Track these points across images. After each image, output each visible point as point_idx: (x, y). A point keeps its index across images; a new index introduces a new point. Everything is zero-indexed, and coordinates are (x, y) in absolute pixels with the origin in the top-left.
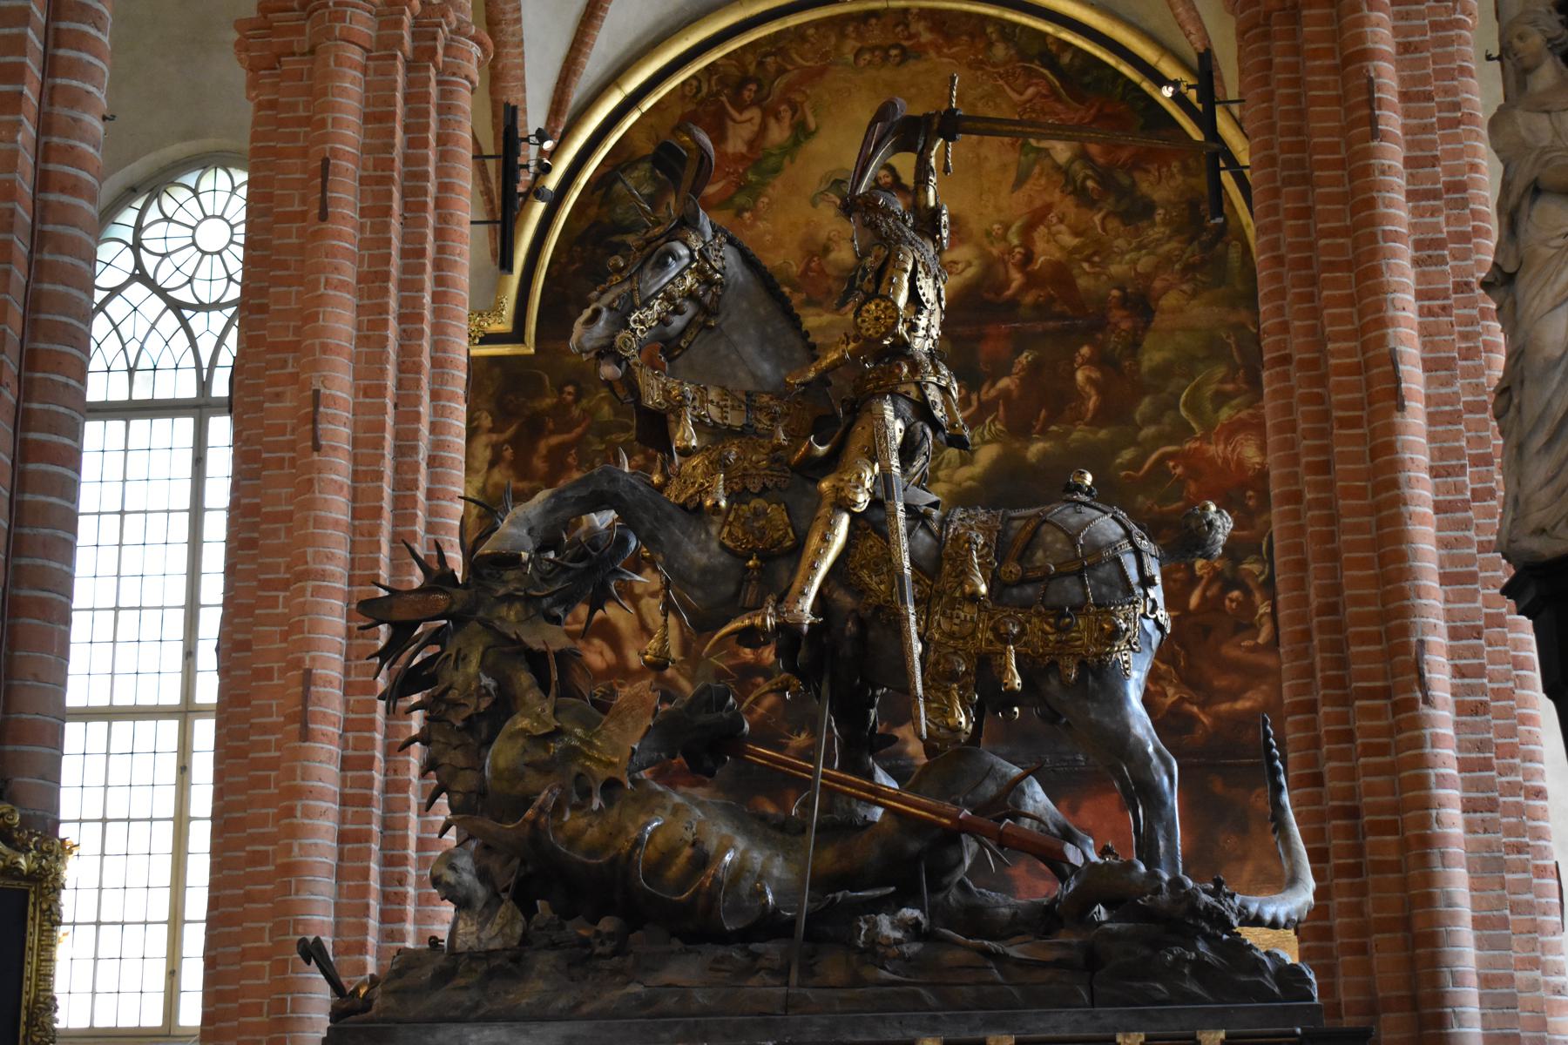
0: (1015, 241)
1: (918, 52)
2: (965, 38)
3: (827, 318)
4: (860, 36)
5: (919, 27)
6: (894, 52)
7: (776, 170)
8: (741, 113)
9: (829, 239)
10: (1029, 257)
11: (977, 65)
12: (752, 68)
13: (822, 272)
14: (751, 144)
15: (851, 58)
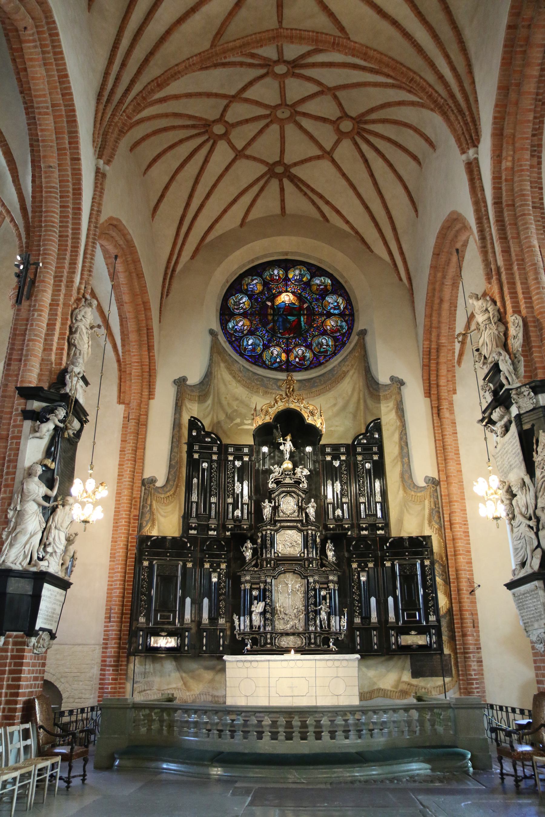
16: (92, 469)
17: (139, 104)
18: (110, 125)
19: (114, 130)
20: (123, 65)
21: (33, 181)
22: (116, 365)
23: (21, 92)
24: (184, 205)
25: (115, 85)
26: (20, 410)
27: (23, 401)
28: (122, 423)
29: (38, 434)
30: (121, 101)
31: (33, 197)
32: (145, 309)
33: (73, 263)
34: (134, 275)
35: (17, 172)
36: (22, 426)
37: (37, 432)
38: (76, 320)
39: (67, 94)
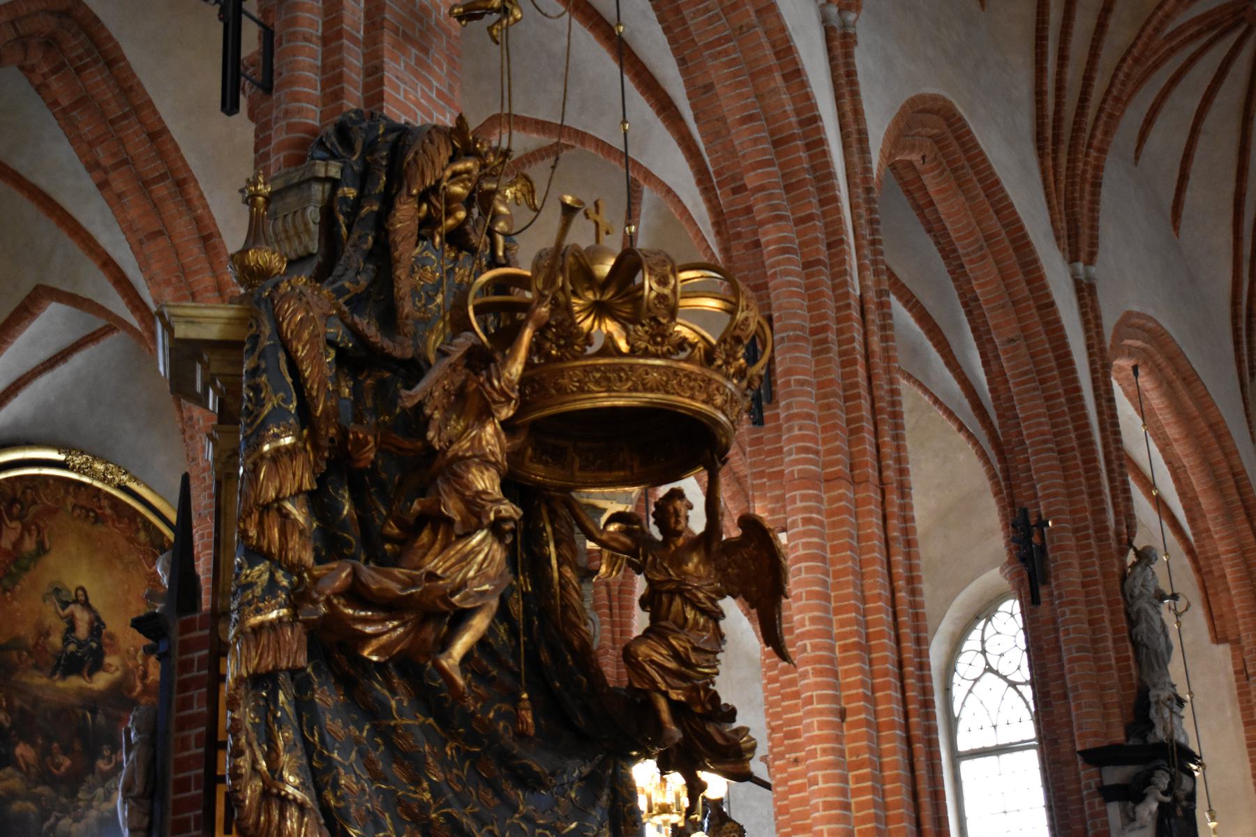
0: (140, 662)
1: (98, 519)
2: (126, 520)
3: (44, 681)
4: (75, 497)
5: (105, 503)
6: (92, 514)
7: (27, 569)
8: (11, 521)
9: (50, 627)
10: (145, 675)
11: (131, 540)
12: (19, 493)
13: (44, 648)
14: (17, 544)
15: (70, 508)
16: (1213, 819)
17: (1111, 116)
18: (1073, 184)
19: (1082, 191)
20: (1063, 58)
21: (986, 364)
22: (1186, 561)
23: (929, 231)
24: (1233, 172)
25: (1059, 104)
26: (1093, 786)
27: (1093, 770)
28: (1235, 685)
29: (1137, 824)
30: (1077, 128)
31: (991, 390)
32: (1219, 437)
33: (1095, 493)
34: (1178, 385)
35: (948, 345)
36: (1105, 813)
37: (1133, 820)
38: (1132, 596)
39: (1004, 209)
